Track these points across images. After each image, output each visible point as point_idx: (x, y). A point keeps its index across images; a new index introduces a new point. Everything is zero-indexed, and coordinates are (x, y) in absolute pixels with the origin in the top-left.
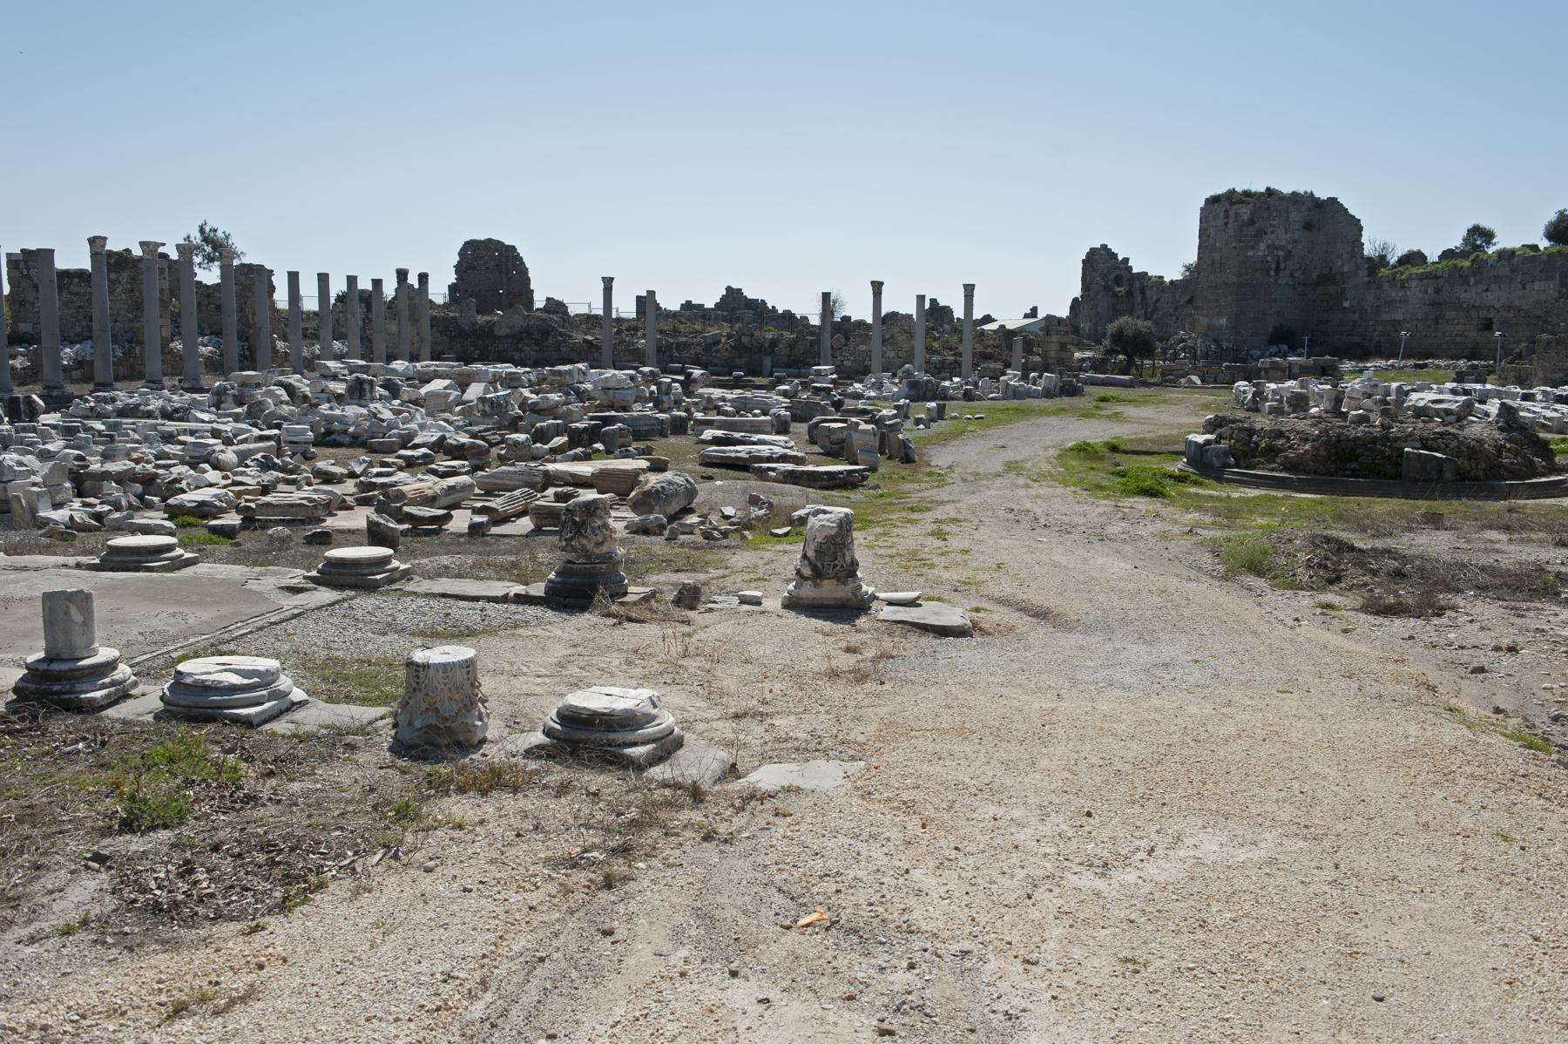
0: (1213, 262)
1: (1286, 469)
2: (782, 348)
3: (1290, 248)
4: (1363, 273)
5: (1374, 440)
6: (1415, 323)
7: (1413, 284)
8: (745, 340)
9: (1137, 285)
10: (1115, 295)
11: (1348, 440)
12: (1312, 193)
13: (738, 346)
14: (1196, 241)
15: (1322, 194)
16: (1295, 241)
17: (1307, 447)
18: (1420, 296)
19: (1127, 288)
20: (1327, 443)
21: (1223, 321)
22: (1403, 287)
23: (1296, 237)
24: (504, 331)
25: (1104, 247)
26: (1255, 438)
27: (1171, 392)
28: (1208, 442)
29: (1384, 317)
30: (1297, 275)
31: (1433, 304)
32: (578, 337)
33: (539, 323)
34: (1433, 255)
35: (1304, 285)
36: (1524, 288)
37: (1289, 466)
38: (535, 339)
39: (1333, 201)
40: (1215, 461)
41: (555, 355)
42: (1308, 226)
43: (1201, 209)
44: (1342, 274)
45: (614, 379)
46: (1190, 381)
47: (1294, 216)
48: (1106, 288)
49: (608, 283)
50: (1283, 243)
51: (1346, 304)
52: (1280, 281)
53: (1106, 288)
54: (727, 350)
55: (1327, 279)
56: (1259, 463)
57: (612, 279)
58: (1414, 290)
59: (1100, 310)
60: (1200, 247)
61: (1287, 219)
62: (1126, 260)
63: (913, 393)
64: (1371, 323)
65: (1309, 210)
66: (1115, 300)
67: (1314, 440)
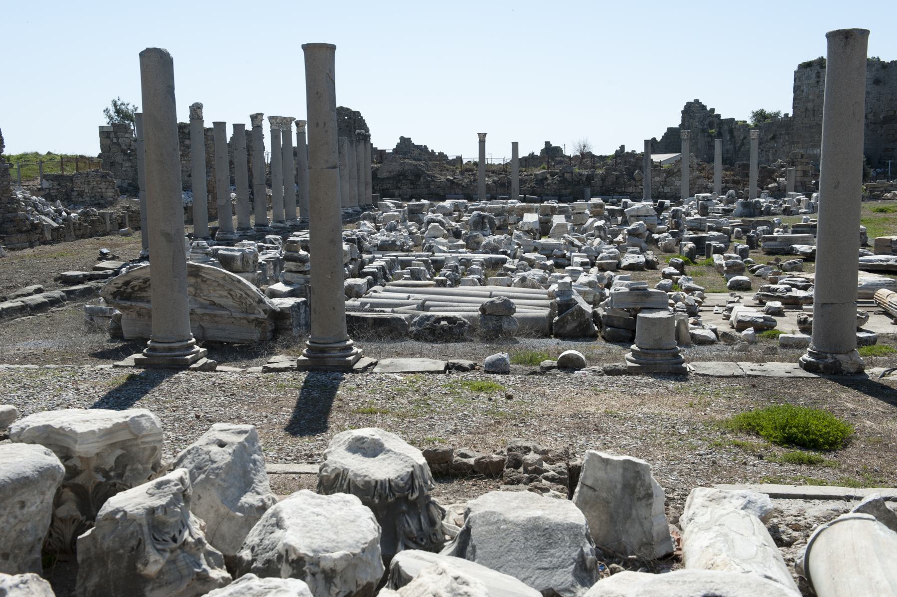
0: (807, 109)
2: (597, 181)
8: (567, 176)
9: (726, 127)
10: (710, 135)
12: (878, 58)
13: (563, 180)
19: (717, 130)
24: (385, 175)
25: (697, 101)
32: (442, 178)
33: (412, 168)
35: (875, 124)
38: (410, 180)
41: (426, 191)
43: (795, 72)
45: (644, 208)
48: (703, 131)
49: (482, 138)
53: (703, 131)
54: (555, 183)
57: (485, 134)
59: (699, 146)
62: (713, 110)
63: (746, 210)
66: (710, 139)
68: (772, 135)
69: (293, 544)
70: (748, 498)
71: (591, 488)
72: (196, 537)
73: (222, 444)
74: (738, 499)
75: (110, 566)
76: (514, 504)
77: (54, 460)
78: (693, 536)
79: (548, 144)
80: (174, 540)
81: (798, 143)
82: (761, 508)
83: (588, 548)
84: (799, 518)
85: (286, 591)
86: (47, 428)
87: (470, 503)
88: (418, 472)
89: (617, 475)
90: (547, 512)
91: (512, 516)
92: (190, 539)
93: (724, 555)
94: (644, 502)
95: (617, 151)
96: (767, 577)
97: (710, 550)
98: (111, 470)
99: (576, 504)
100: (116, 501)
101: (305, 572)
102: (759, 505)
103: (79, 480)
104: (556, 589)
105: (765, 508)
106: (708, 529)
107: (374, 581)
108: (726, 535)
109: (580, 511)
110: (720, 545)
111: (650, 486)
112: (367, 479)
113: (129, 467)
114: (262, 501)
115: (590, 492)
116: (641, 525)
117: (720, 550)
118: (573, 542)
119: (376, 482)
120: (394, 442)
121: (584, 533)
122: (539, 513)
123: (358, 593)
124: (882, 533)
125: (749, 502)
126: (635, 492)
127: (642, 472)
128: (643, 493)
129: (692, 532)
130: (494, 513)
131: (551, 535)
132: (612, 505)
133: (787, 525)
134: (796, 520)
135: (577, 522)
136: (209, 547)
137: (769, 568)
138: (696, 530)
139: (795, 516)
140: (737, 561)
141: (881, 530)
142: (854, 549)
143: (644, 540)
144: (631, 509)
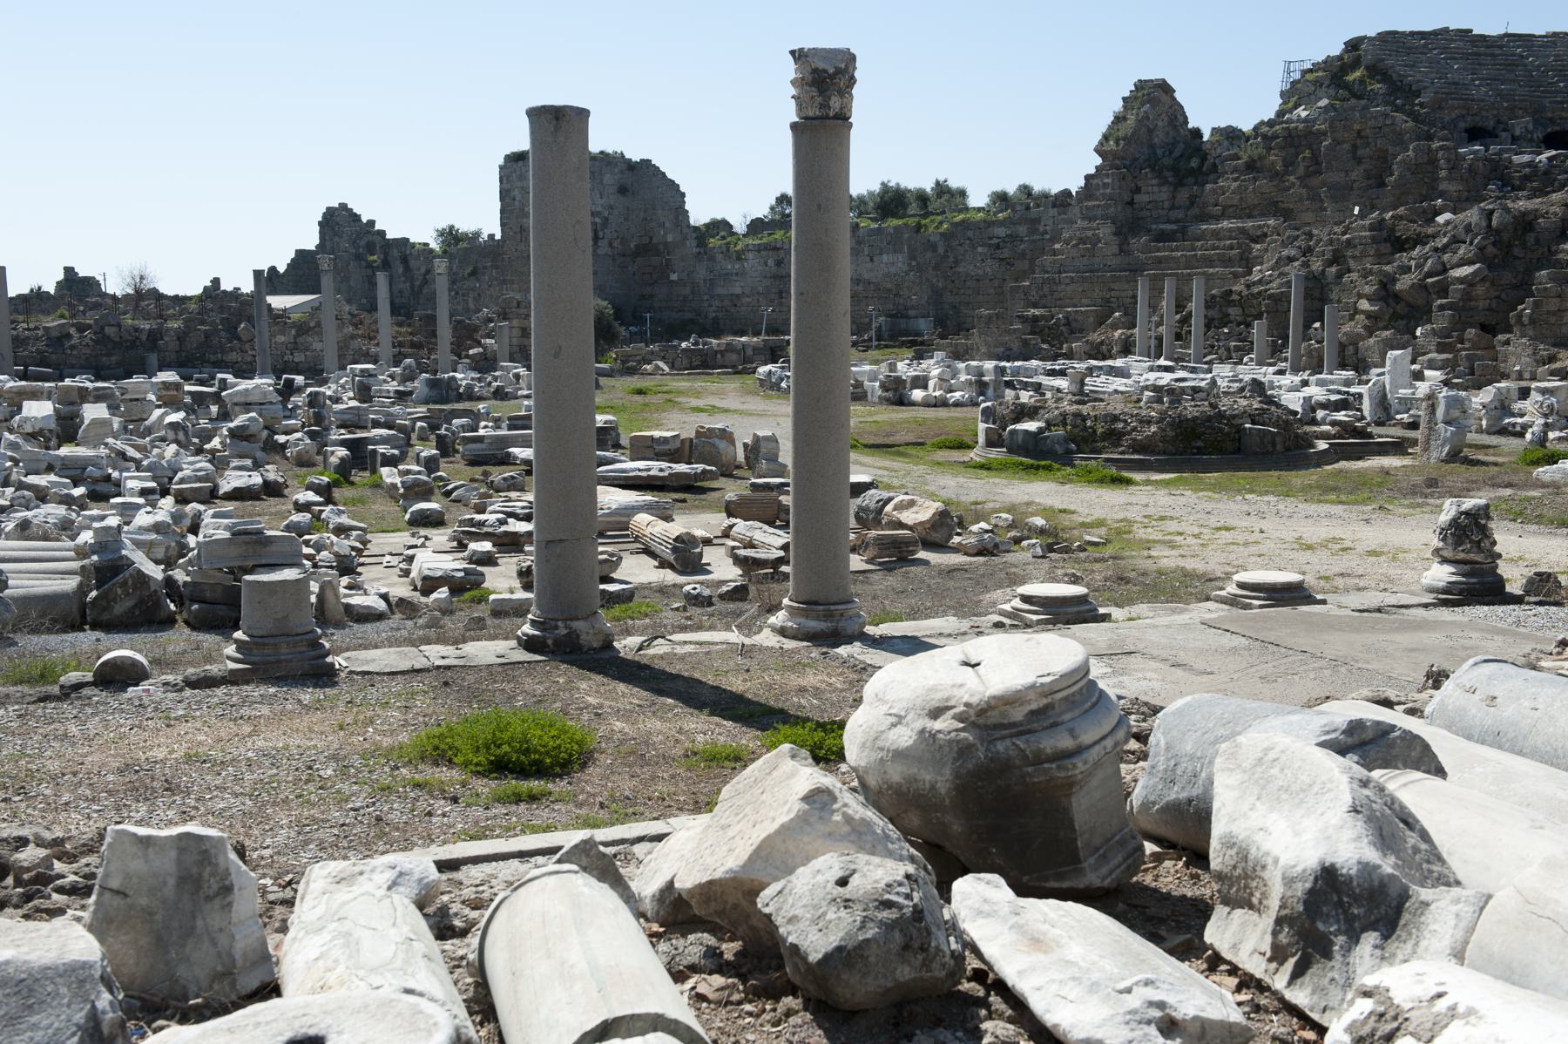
1: (1135, 452)
2: (169, 342)
3: (606, 214)
4: (692, 244)
5: (1209, 419)
6: (756, 297)
7: (750, 255)
8: (110, 331)
9: (395, 253)
10: (370, 265)
11: (1188, 420)
13: (102, 339)
14: (498, 204)
15: (634, 155)
16: (611, 207)
17: (1153, 429)
18: (760, 268)
20: (1171, 424)
22: (739, 259)
23: (612, 202)
25: (343, 206)
26: (1089, 423)
27: (678, 381)
28: (1041, 431)
29: (720, 291)
30: (615, 244)
31: (775, 277)
34: (740, 226)
36: (872, 260)
37: (1137, 447)
39: (646, 163)
40: (1060, 450)
42: (623, 190)
43: (501, 167)
44: (666, 244)
45: (258, 390)
46: (658, 367)
47: (608, 178)
50: (599, 209)
51: (674, 277)
52: (600, 251)
54: (87, 344)
55: (647, 249)
56: (1104, 447)
58: (752, 261)
60: (502, 211)
61: (601, 183)
62: (372, 223)
63: (434, 393)
64: (706, 297)
65: (622, 172)
66: (369, 272)
67: (1157, 423)
68: (470, 269)
70: (398, 869)
71: (117, 892)
74: (382, 872)
78: (296, 945)
79: (69, 271)
81: (512, 282)
82: (420, 880)
83: (104, 1000)
84: (481, 888)
89: (166, 863)
90: (24, 949)
93: (341, 969)
94: (217, 903)
95: (205, 288)
96: (408, 991)
97: (321, 963)
99: (91, 928)
102: (416, 876)
105: (426, 881)
109: (91, 938)
111: (227, 873)
115: (118, 901)
116: (214, 942)
117: (336, 961)
118: (76, 995)
121: (97, 974)
124: (586, 890)
125: (401, 874)
127: (213, 851)
128: (215, 887)
131: (31, 990)
132: (158, 917)
133: (463, 902)
134: (477, 892)
135: (84, 959)
137: (413, 975)
138: (301, 935)
139: (477, 886)
140: (361, 973)
141: (585, 885)
142: (544, 922)
143: (220, 968)
144: (194, 918)
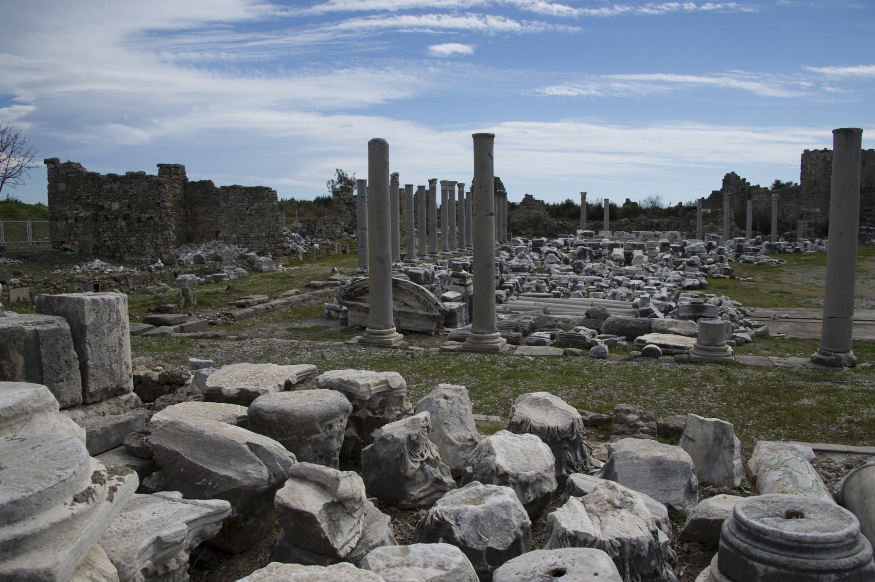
14: (800, 171)
21: (818, 210)
25: (733, 173)
43: (802, 155)
57: (586, 193)
60: (801, 174)
62: (744, 180)
69: (501, 464)
72: (435, 455)
73: (446, 398)
75: (383, 469)
76: (642, 447)
77: (345, 401)
78: (766, 473)
79: (628, 200)
80: (422, 456)
83: (694, 479)
85: (503, 494)
86: (342, 381)
87: (613, 445)
88: (576, 421)
89: (710, 432)
91: (642, 455)
92: (431, 457)
93: (790, 486)
94: (727, 451)
97: (780, 482)
98: (376, 409)
100: (387, 429)
101: (509, 483)
102: (806, 454)
103: (358, 414)
104: (671, 504)
106: (777, 469)
107: (551, 491)
108: (790, 473)
110: (787, 480)
112: (542, 425)
113: (386, 409)
114: (471, 435)
116: (725, 464)
117: (787, 483)
119: (549, 428)
120: (558, 402)
122: (660, 454)
123: (542, 498)
126: (722, 443)
128: (728, 444)
129: (764, 471)
130: (630, 452)
133: (823, 468)
136: (441, 463)
138: (768, 469)
140: (800, 490)
143: (727, 475)
144: (719, 454)
